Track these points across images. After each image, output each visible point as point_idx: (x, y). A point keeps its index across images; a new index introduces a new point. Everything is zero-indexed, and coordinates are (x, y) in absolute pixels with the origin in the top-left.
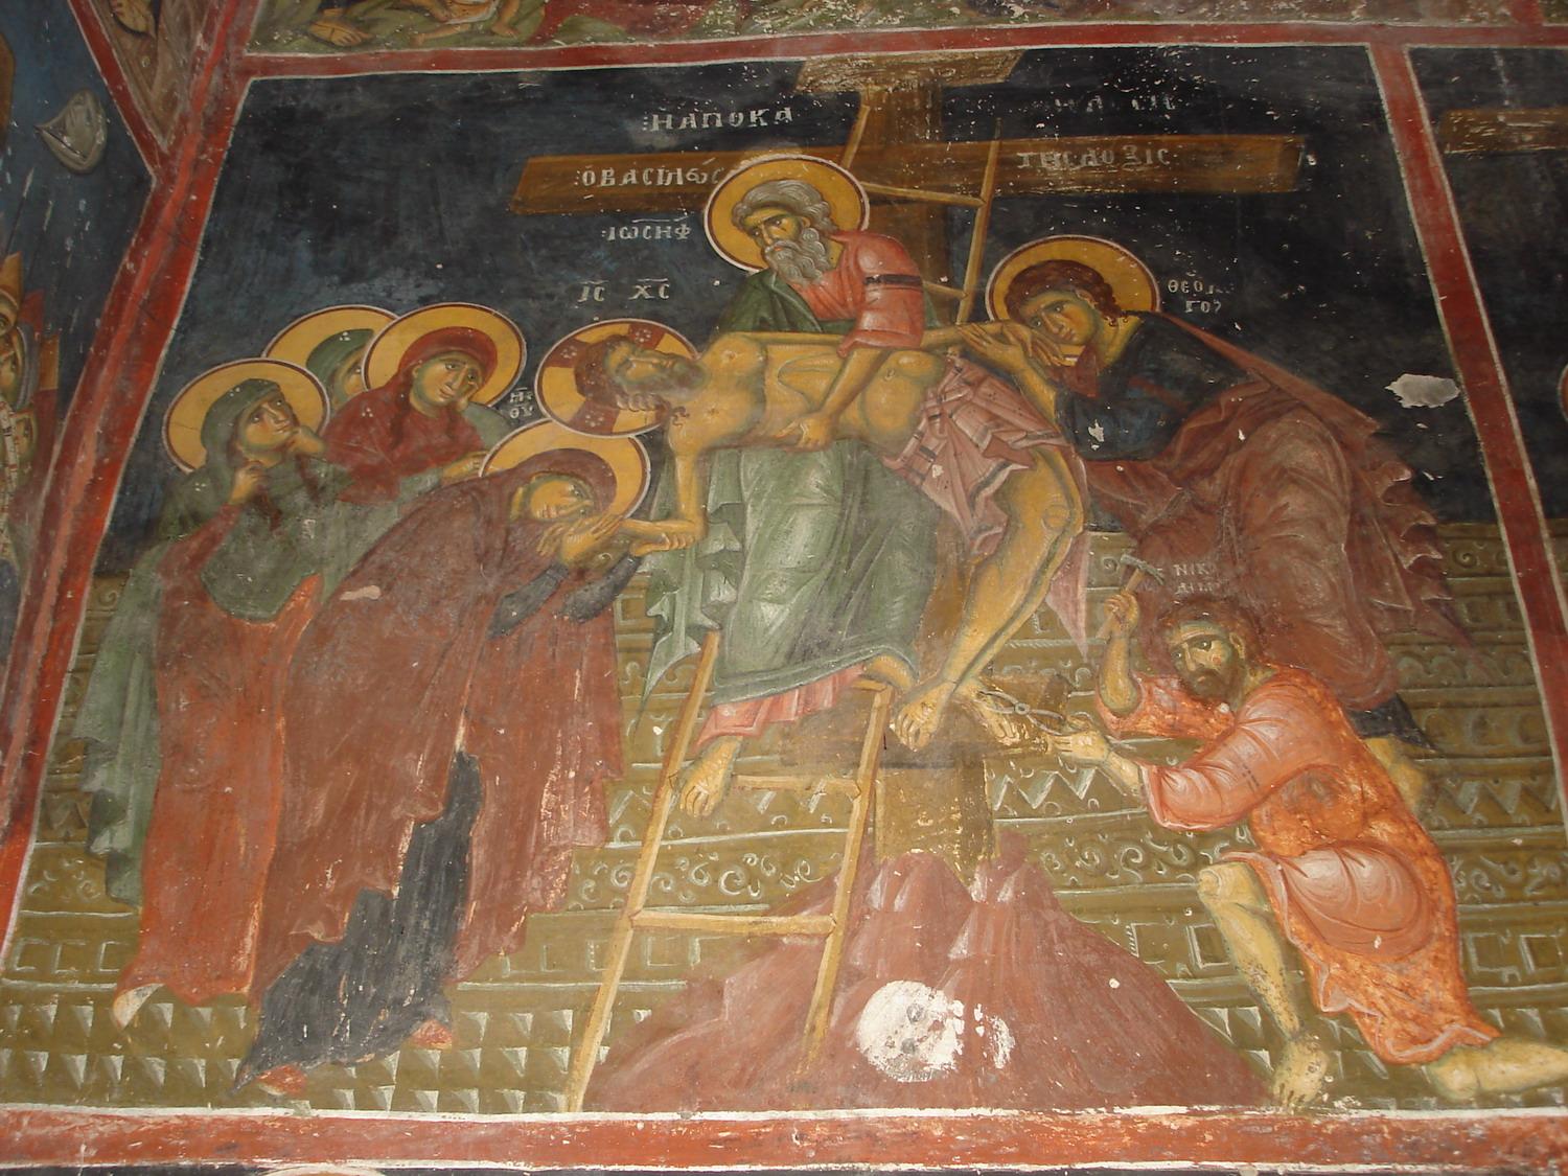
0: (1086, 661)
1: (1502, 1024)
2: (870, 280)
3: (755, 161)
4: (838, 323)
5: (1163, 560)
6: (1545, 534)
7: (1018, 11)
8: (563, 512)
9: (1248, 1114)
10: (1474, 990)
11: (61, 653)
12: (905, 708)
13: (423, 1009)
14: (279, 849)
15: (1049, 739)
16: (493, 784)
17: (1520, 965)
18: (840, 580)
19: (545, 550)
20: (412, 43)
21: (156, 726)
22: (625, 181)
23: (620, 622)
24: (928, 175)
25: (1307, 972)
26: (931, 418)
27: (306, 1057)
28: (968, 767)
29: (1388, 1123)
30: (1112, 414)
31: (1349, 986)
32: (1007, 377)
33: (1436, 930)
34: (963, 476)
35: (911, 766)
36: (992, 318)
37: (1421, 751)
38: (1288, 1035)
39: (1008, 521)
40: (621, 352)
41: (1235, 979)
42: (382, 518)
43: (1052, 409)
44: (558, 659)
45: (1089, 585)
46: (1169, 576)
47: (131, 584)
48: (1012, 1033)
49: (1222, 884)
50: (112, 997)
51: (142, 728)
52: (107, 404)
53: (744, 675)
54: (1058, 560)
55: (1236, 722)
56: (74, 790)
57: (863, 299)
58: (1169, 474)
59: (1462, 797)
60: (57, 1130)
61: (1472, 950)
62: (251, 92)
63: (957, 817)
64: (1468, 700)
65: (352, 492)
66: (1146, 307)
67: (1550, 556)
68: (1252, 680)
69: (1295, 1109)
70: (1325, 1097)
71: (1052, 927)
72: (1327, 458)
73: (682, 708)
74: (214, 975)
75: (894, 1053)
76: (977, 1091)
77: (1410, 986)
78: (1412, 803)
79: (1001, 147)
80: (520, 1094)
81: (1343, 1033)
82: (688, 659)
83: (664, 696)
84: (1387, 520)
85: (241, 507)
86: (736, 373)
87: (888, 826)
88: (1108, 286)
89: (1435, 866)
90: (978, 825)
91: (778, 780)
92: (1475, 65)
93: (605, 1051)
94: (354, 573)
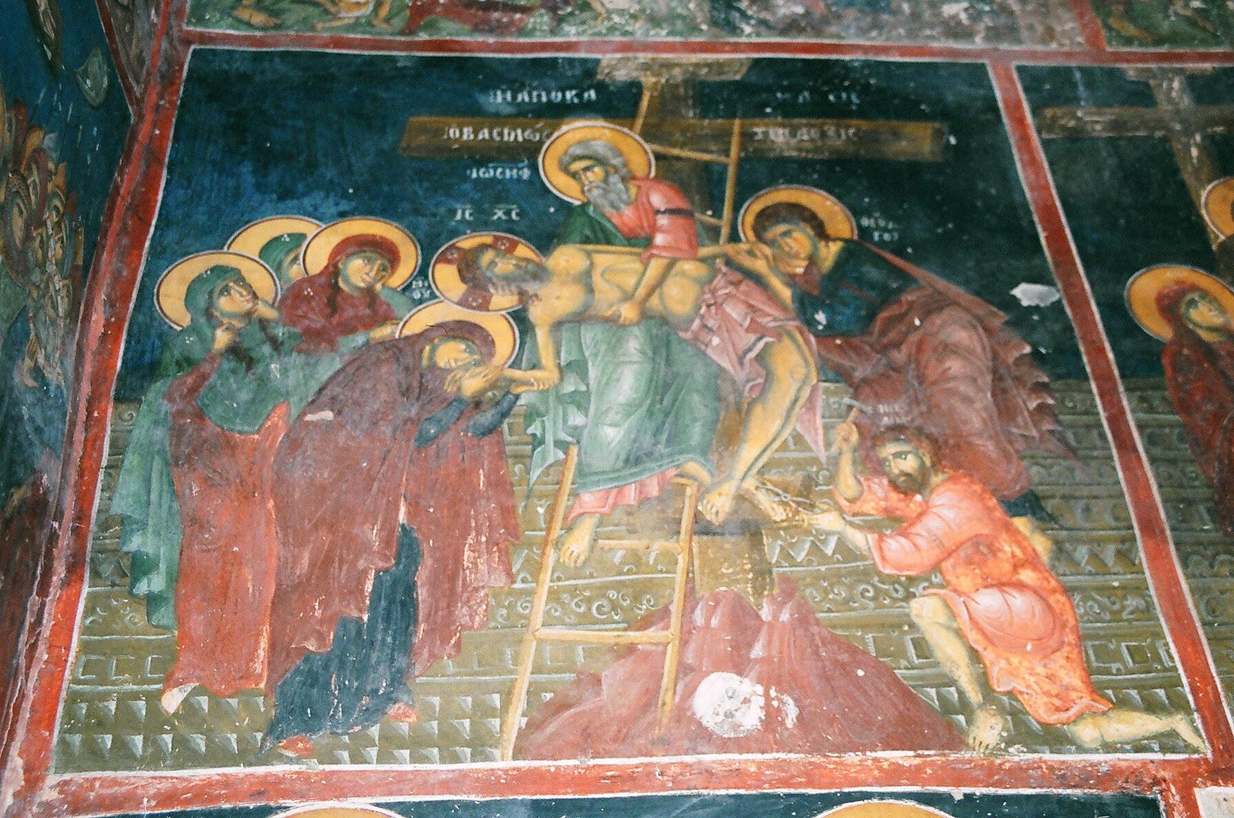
2: (658, 212)
4: (640, 240)
6: (1121, 388)
7: (748, 29)
8: (459, 363)
9: (953, 757)
11: (95, 455)
13: (394, 696)
14: (277, 590)
15: (805, 517)
16: (427, 546)
18: (656, 411)
19: (450, 389)
20: (313, 28)
21: (176, 506)
22: (480, 137)
23: (507, 437)
24: (695, 141)
25: (985, 667)
26: (709, 306)
27: (312, 730)
29: (1045, 762)
31: (1012, 674)
33: (1066, 639)
34: (734, 345)
35: (714, 534)
37: (1049, 526)
39: (767, 375)
40: (488, 257)
42: (328, 366)
44: (467, 462)
45: (823, 417)
46: (876, 413)
47: (144, 407)
49: (926, 610)
50: (160, 693)
51: (165, 506)
52: (107, 280)
53: (596, 474)
54: (802, 401)
55: (928, 507)
56: (115, 551)
57: (655, 224)
58: (871, 346)
60: (124, 789)
61: (1091, 652)
62: (192, 56)
63: (748, 567)
64: (1078, 494)
65: (304, 346)
66: (847, 235)
67: (1125, 403)
68: (936, 479)
70: (1003, 746)
71: (817, 638)
72: (975, 337)
73: (556, 495)
74: (237, 676)
78: (1045, 558)
79: (742, 126)
80: (468, 751)
82: (557, 463)
83: (543, 487)
85: (222, 355)
86: (572, 272)
87: (702, 573)
89: (1063, 599)
90: (762, 572)
91: (627, 543)
92: (1061, 76)
93: (524, 720)
94: (313, 402)
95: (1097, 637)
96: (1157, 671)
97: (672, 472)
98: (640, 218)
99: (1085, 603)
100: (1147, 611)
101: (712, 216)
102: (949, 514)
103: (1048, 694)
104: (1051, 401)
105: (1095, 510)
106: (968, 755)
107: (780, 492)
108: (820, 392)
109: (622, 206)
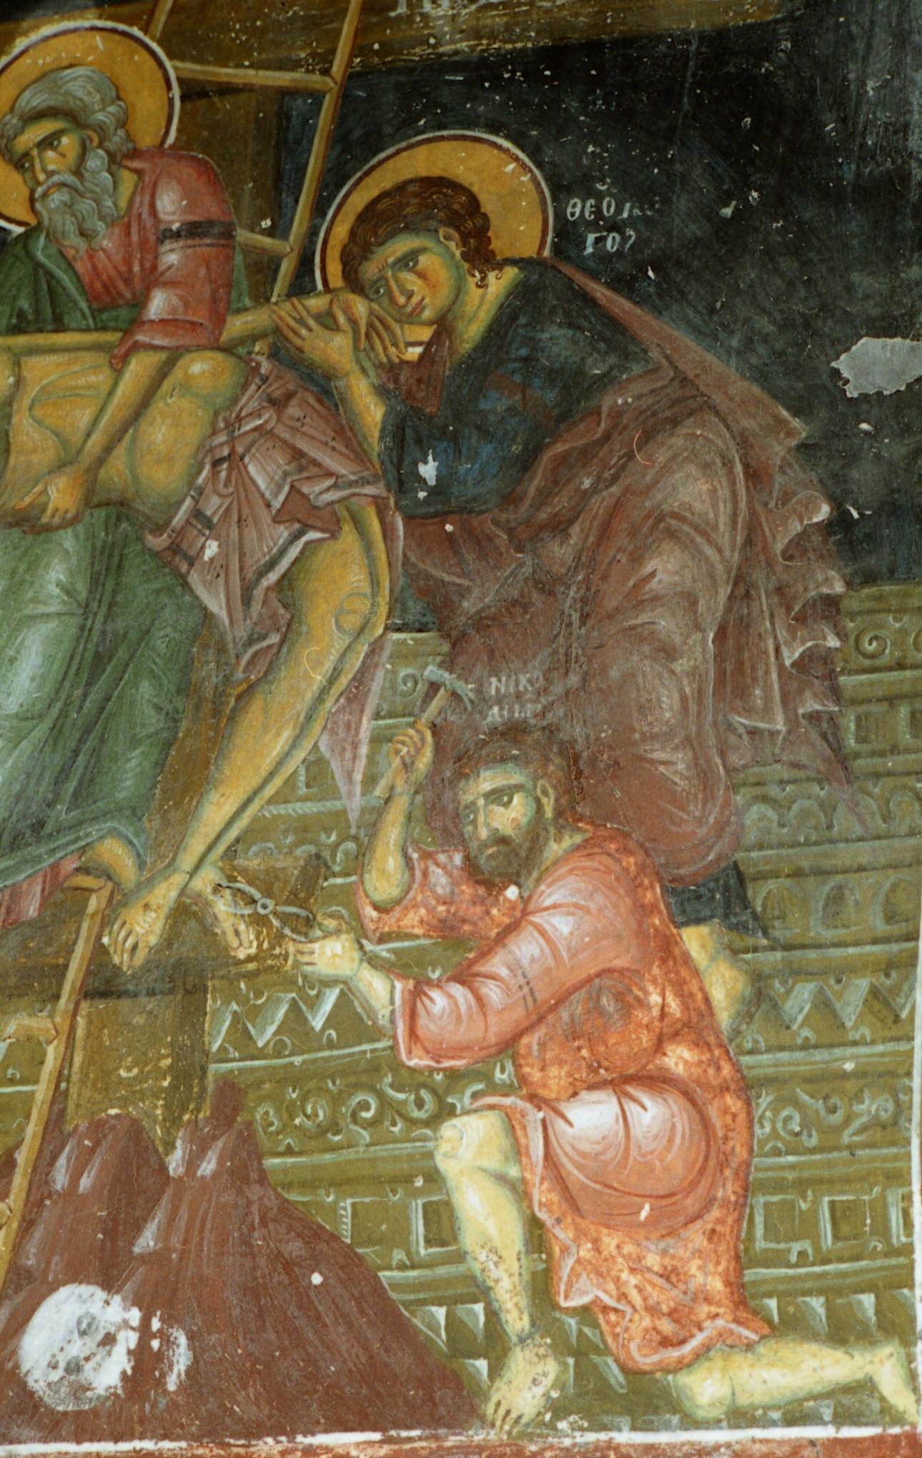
0: (353, 831)
1: (776, 1318)
3: (34, 37)
4: (113, 308)
5: (479, 670)
9: (453, 1440)
10: (751, 1274)
12: (125, 914)
15: (291, 948)
17: (816, 1239)
18: (67, 728)
26: (216, 463)
28: (188, 992)
29: (617, 1448)
30: (455, 439)
32: (322, 385)
33: (720, 1194)
34: (242, 556)
36: (320, 286)
37: (750, 941)
38: (514, 1339)
39: (289, 625)
41: (462, 1268)
43: (377, 434)
45: (377, 716)
48: (191, 1347)
54: (344, 681)
55: (525, 913)
58: (511, 532)
59: (789, 1006)
61: (759, 1220)
63: (167, 1062)
64: (827, 864)
66: (528, 249)
69: (509, 1433)
70: (548, 1417)
71: (255, 1208)
72: (724, 492)
75: (55, 1376)
76: (142, 1421)
77: (674, 1269)
78: (724, 1018)
81: (580, 1332)
84: (780, 590)
87: (83, 1081)
88: (485, 215)
95: (779, 1186)
96: (873, 1255)
97: (70, 865)
98: (128, 262)
99: (776, 1112)
100: (889, 1129)
101: (270, 233)
102: (562, 925)
103: (653, 1310)
104: (833, 642)
105: (850, 901)
106: (479, 1436)
107: (257, 895)
108: (387, 653)
109: (100, 226)
